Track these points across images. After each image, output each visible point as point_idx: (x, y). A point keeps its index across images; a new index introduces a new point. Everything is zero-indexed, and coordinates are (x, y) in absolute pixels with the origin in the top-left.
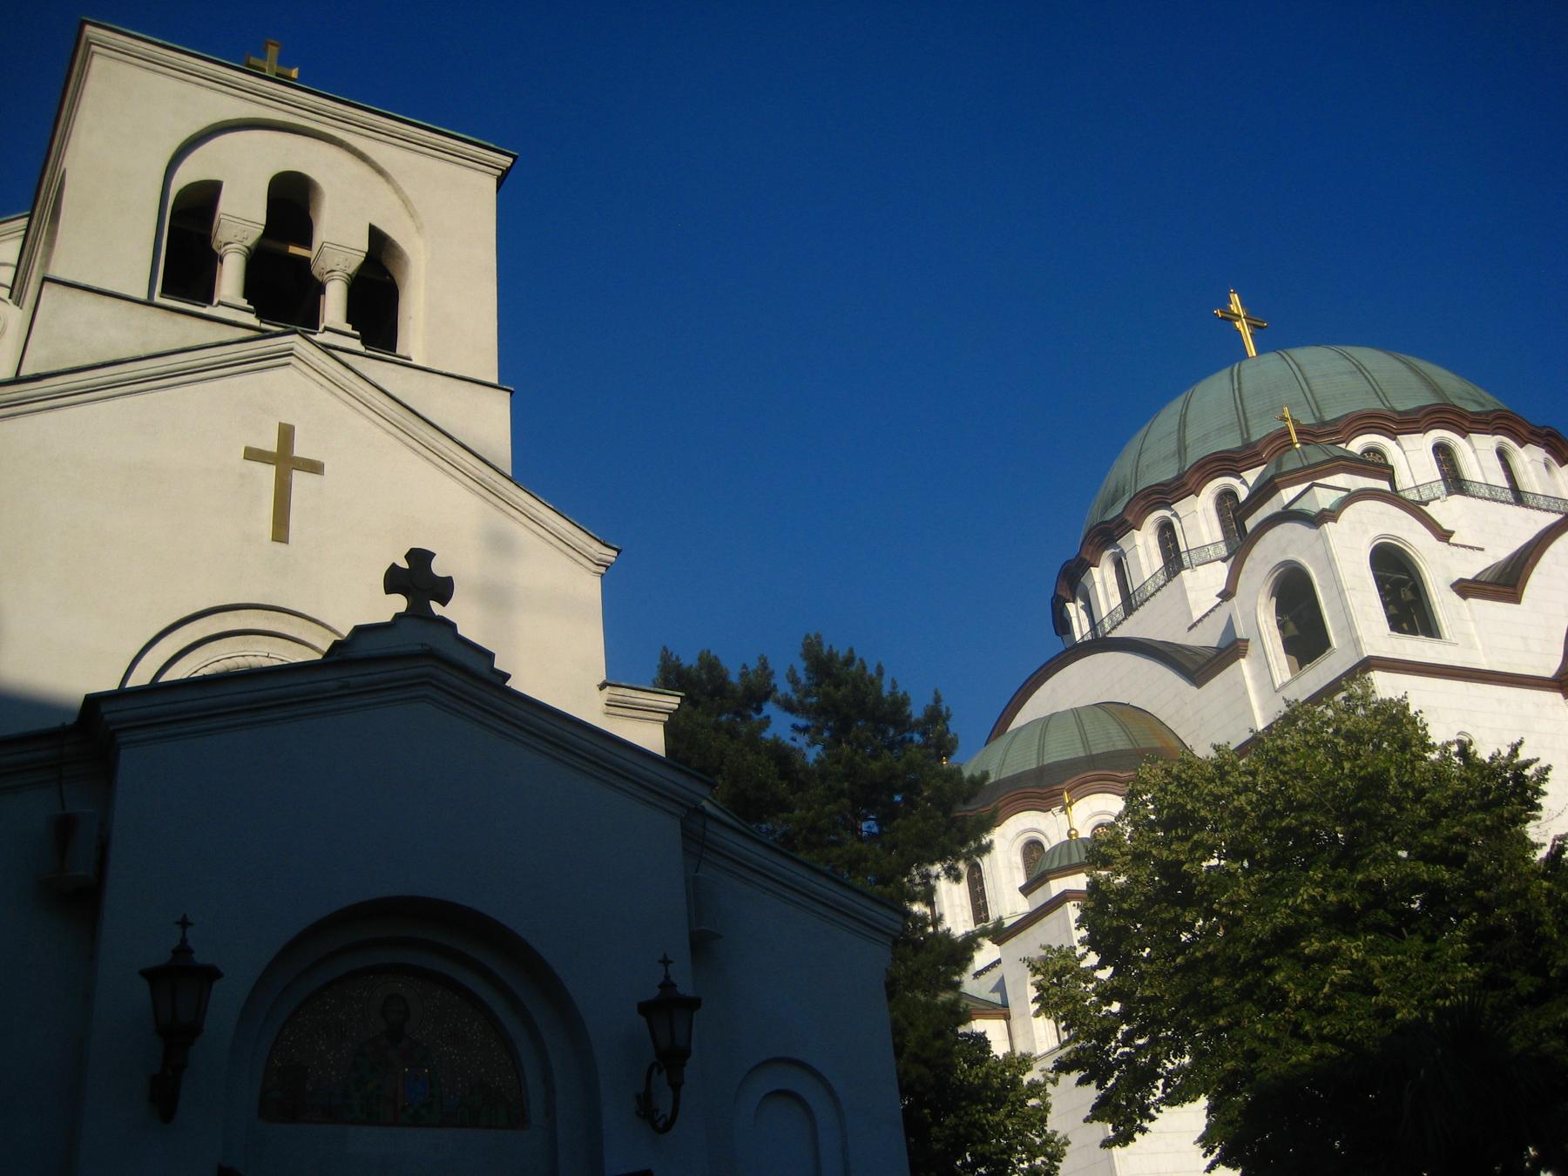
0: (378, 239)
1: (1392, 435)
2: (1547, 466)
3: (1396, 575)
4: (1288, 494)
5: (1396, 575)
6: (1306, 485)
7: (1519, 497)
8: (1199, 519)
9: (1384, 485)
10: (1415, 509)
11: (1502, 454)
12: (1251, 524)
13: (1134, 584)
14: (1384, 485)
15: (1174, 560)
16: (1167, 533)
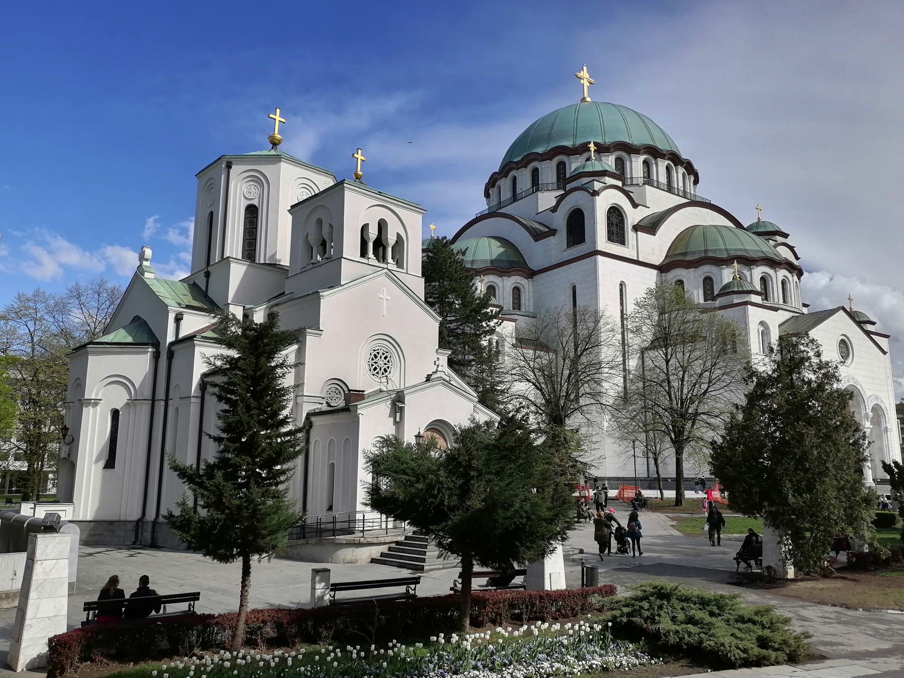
0: (398, 235)
1: (629, 154)
2: (684, 174)
3: (615, 215)
4: (585, 180)
5: (615, 215)
6: (592, 179)
7: (670, 189)
8: (548, 172)
9: (619, 184)
10: (627, 194)
11: (668, 169)
12: (568, 187)
13: (518, 191)
14: (619, 184)
15: (536, 184)
16: (535, 173)
